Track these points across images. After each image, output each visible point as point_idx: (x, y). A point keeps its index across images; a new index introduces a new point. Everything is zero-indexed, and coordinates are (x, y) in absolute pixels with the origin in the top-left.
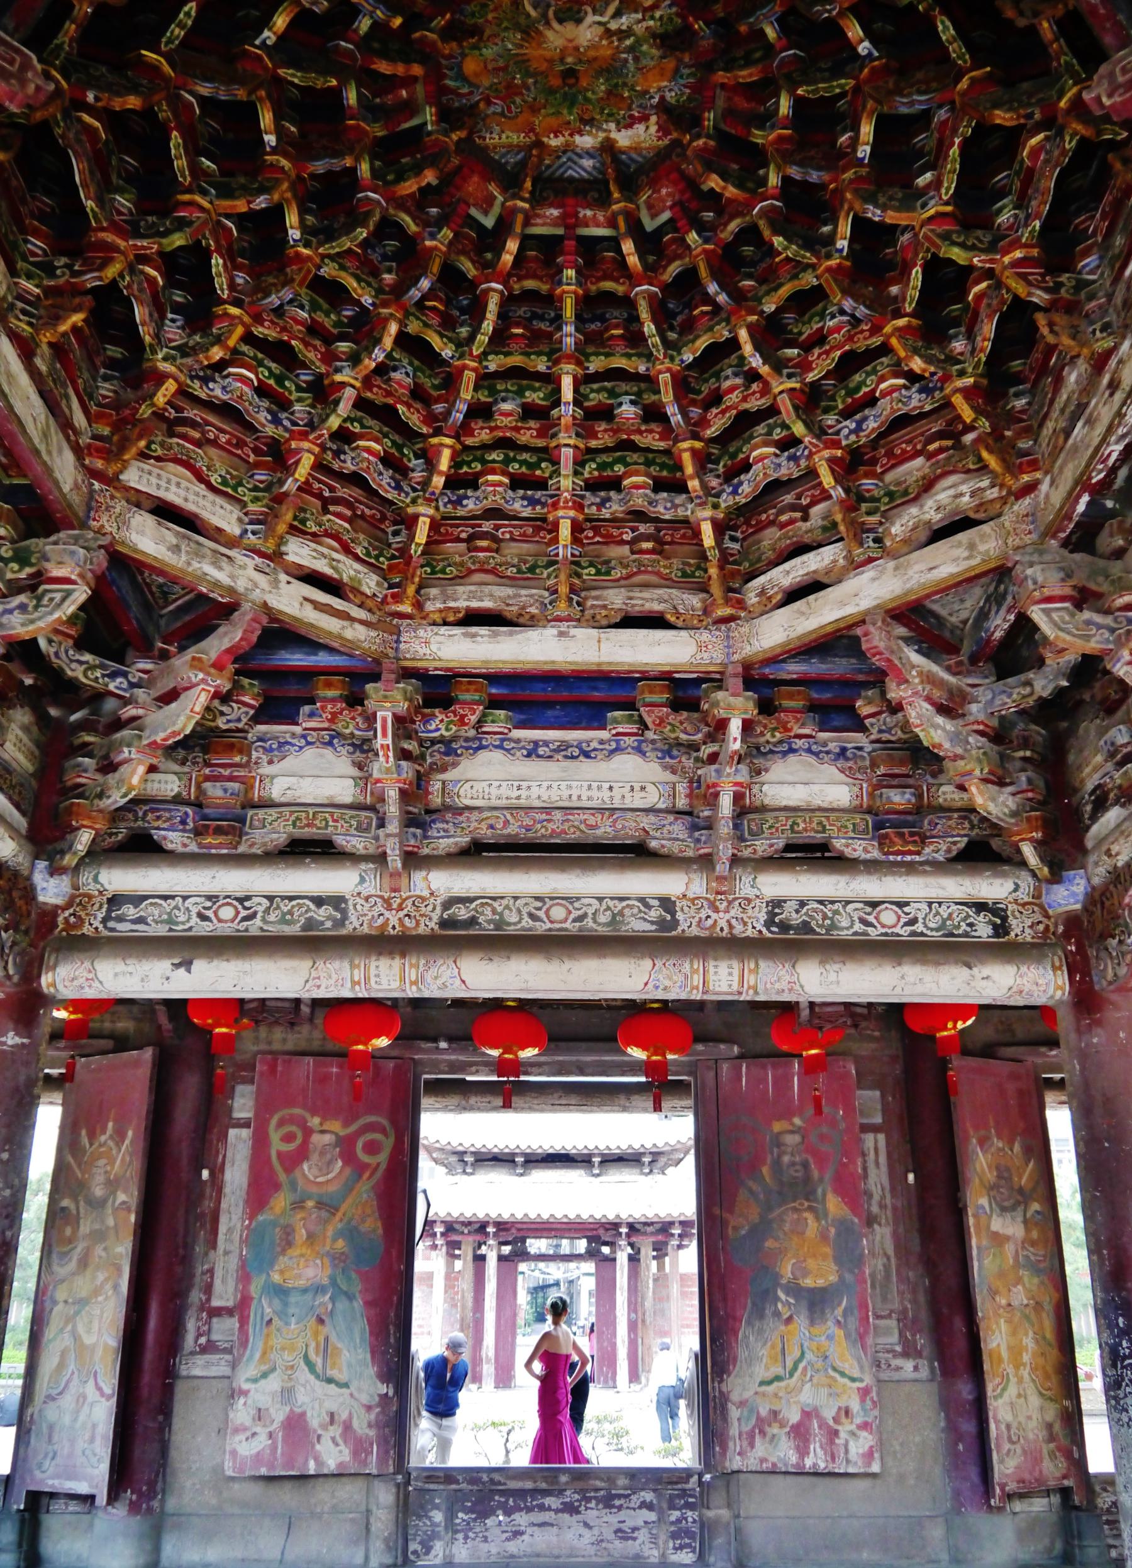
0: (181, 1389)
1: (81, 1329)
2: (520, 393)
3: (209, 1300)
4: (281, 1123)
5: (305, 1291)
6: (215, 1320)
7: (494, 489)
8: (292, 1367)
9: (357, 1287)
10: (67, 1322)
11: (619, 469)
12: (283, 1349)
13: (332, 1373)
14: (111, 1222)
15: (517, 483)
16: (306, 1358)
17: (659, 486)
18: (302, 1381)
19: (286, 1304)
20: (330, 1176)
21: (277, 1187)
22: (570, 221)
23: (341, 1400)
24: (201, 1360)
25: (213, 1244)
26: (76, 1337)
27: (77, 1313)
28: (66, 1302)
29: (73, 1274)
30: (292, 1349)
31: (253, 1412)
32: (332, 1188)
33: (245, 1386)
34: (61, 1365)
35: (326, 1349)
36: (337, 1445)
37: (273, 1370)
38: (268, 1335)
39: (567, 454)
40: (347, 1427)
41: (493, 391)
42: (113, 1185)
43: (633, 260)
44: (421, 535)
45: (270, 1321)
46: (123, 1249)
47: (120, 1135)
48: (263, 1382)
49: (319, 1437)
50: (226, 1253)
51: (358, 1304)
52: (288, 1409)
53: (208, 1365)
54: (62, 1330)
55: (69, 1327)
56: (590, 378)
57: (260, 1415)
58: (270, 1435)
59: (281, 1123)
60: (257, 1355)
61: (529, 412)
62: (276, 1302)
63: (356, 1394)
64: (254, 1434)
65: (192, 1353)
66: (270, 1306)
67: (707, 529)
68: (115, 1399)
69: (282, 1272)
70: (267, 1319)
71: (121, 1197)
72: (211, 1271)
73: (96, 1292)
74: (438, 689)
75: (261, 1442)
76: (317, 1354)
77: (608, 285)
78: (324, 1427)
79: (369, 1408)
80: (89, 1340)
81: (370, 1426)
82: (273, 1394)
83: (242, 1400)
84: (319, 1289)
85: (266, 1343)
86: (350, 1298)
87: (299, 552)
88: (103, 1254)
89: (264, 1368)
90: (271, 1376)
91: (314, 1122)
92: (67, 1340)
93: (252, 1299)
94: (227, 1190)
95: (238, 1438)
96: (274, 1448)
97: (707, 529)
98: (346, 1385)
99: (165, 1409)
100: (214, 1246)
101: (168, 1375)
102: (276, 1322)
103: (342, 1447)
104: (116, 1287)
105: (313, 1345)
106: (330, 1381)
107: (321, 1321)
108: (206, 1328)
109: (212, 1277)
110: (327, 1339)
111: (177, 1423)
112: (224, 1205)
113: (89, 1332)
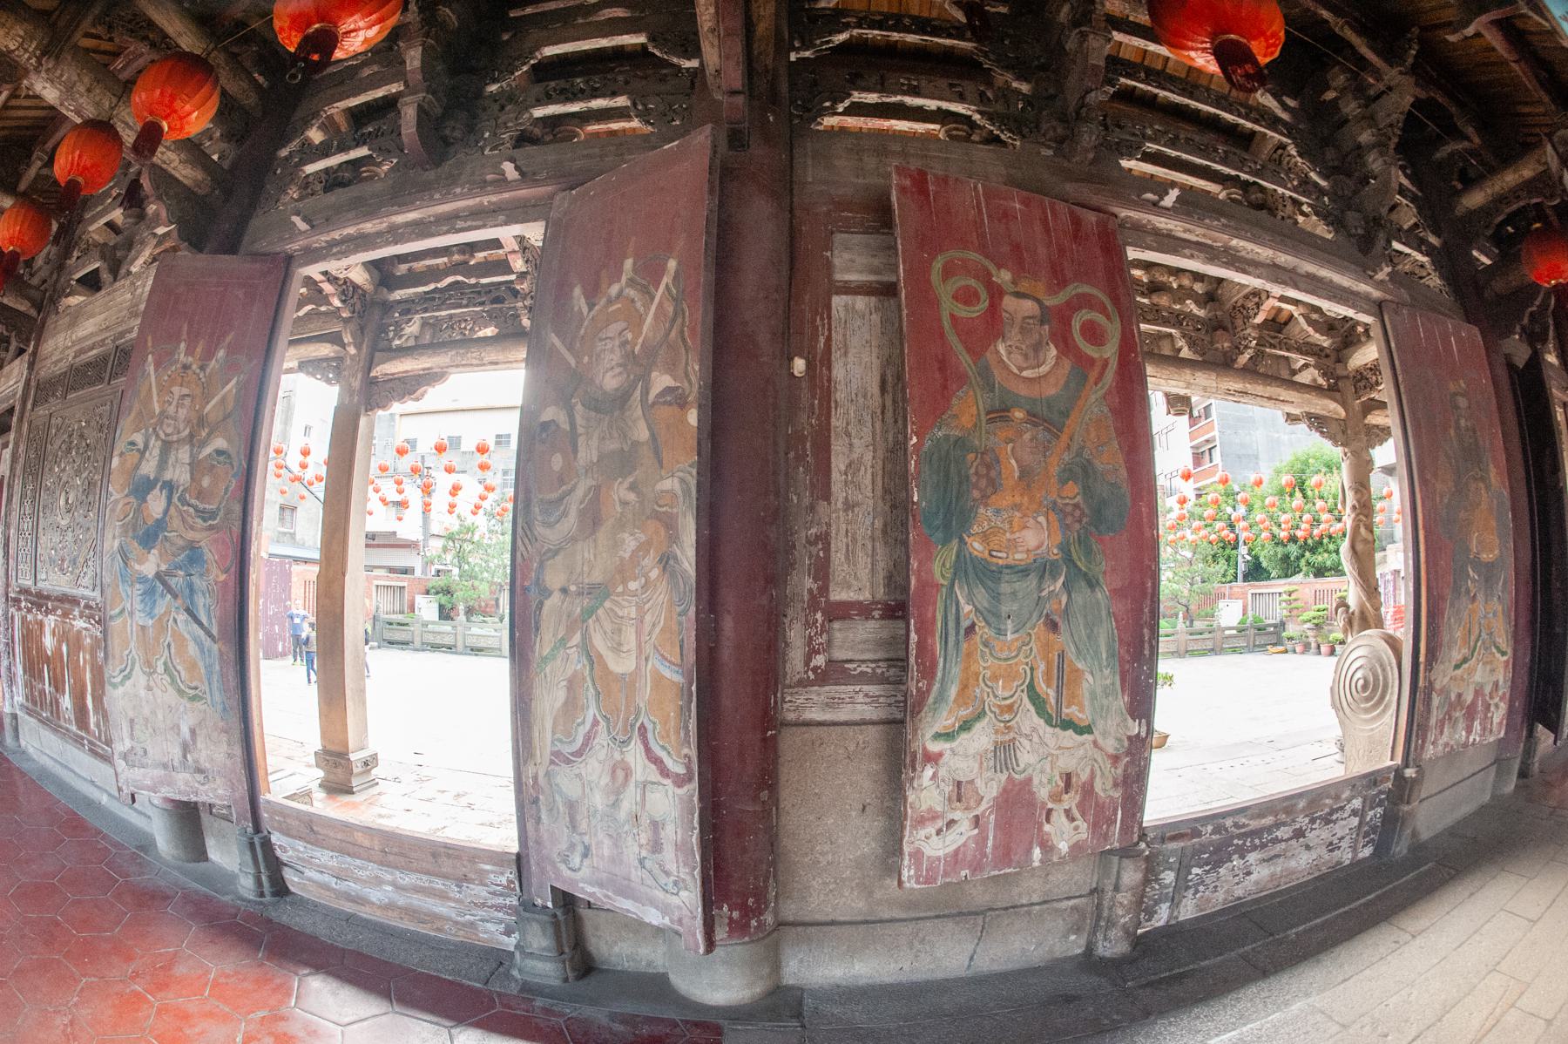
0: (789, 742)
1: (599, 642)
3: (824, 590)
4: (947, 273)
5: (1024, 572)
6: (836, 625)
8: (1010, 708)
9: (1101, 566)
10: (571, 630)
12: (995, 678)
13: (1071, 711)
14: (642, 433)
16: (1031, 688)
18: (1026, 730)
19: (996, 597)
20: (1044, 369)
21: (962, 379)
23: (1081, 752)
24: (820, 694)
25: (823, 491)
26: (593, 659)
27: (590, 612)
28: (564, 591)
29: (574, 540)
30: (1010, 676)
31: (948, 789)
32: (1051, 390)
33: (934, 747)
34: (571, 706)
35: (1063, 675)
36: (1073, 820)
37: (980, 715)
38: (969, 655)
40: (1088, 790)
42: (639, 364)
45: (971, 629)
46: (677, 482)
47: (650, 273)
48: (964, 735)
49: (1049, 811)
50: (849, 506)
51: (1101, 595)
52: (1004, 777)
53: (831, 704)
54: (563, 642)
55: (577, 638)
57: (960, 792)
58: (977, 821)
59: (947, 273)
60: (953, 691)
62: (982, 596)
63: (1100, 741)
64: (951, 823)
65: (803, 683)
66: (970, 600)
68: (695, 784)
69: (985, 537)
70: (965, 624)
71: (661, 381)
72: (824, 539)
73: (624, 572)
75: (963, 833)
76: (1048, 686)
78: (1056, 797)
79: (1115, 759)
80: (622, 665)
81: (1116, 785)
82: (981, 756)
83: (929, 772)
84: (1045, 569)
85: (966, 669)
86: (1092, 584)
88: (632, 497)
89: (964, 713)
90: (978, 726)
91: (1004, 277)
92: (575, 663)
93: (938, 586)
94: (840, 395)
95: (922, 833)
96: (981, 840)
98: (1088, 730)
99: (767, 780)
100: (827, 496)
101: (768, 723)
102: (983, 631)
103: (1080, 822)
104: (666, 561)
105: (1042, 667)
106: (1067, 724)
107: (1053, 626)
108: (823, 639)
109: (827, 549)
110: (1062, 656)
111: (787, 797)
112: (837, 422)
113: (617, 648)
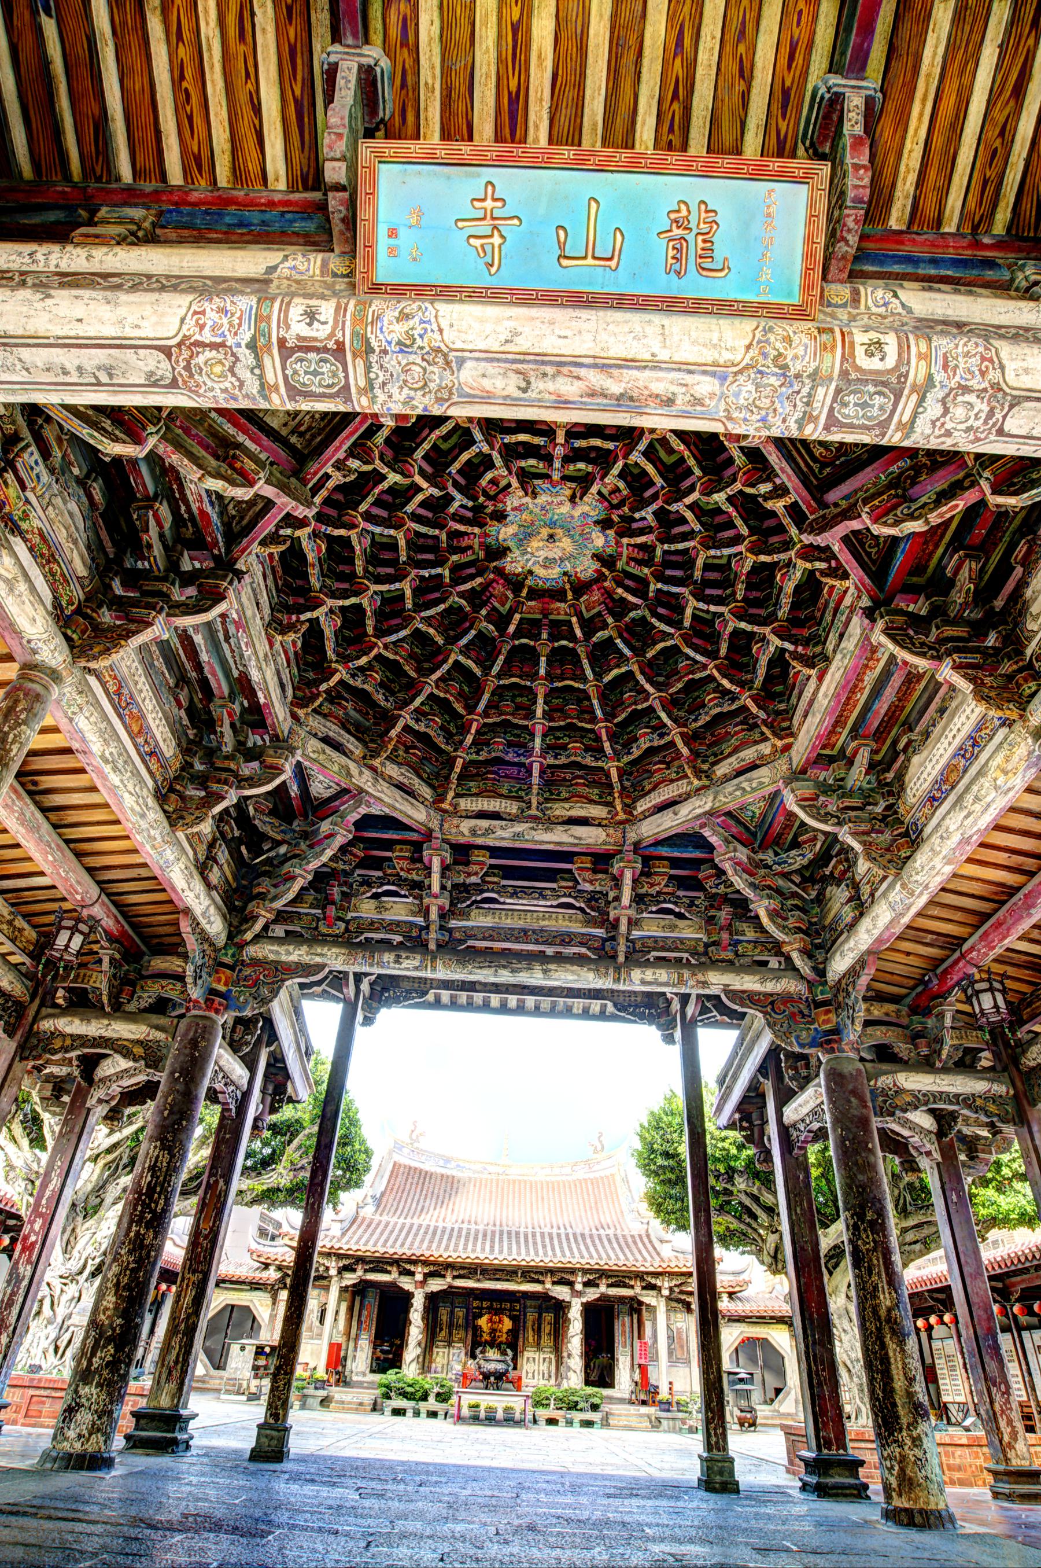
2: (514, 696)
7: (499, 746)
11: (567, 740)
15: (510, 744)
17: (587, 749)
22: (545, 613)
39: (539, 729)
41: (501, 696)
43: (578, 633)
44: (457, 770)
56: (553, 690)
61: (519, 707)
67: (614, 773)
74: (462, 852)
77: (564, 643)
87: (392, 770)
97: (614, 773)
